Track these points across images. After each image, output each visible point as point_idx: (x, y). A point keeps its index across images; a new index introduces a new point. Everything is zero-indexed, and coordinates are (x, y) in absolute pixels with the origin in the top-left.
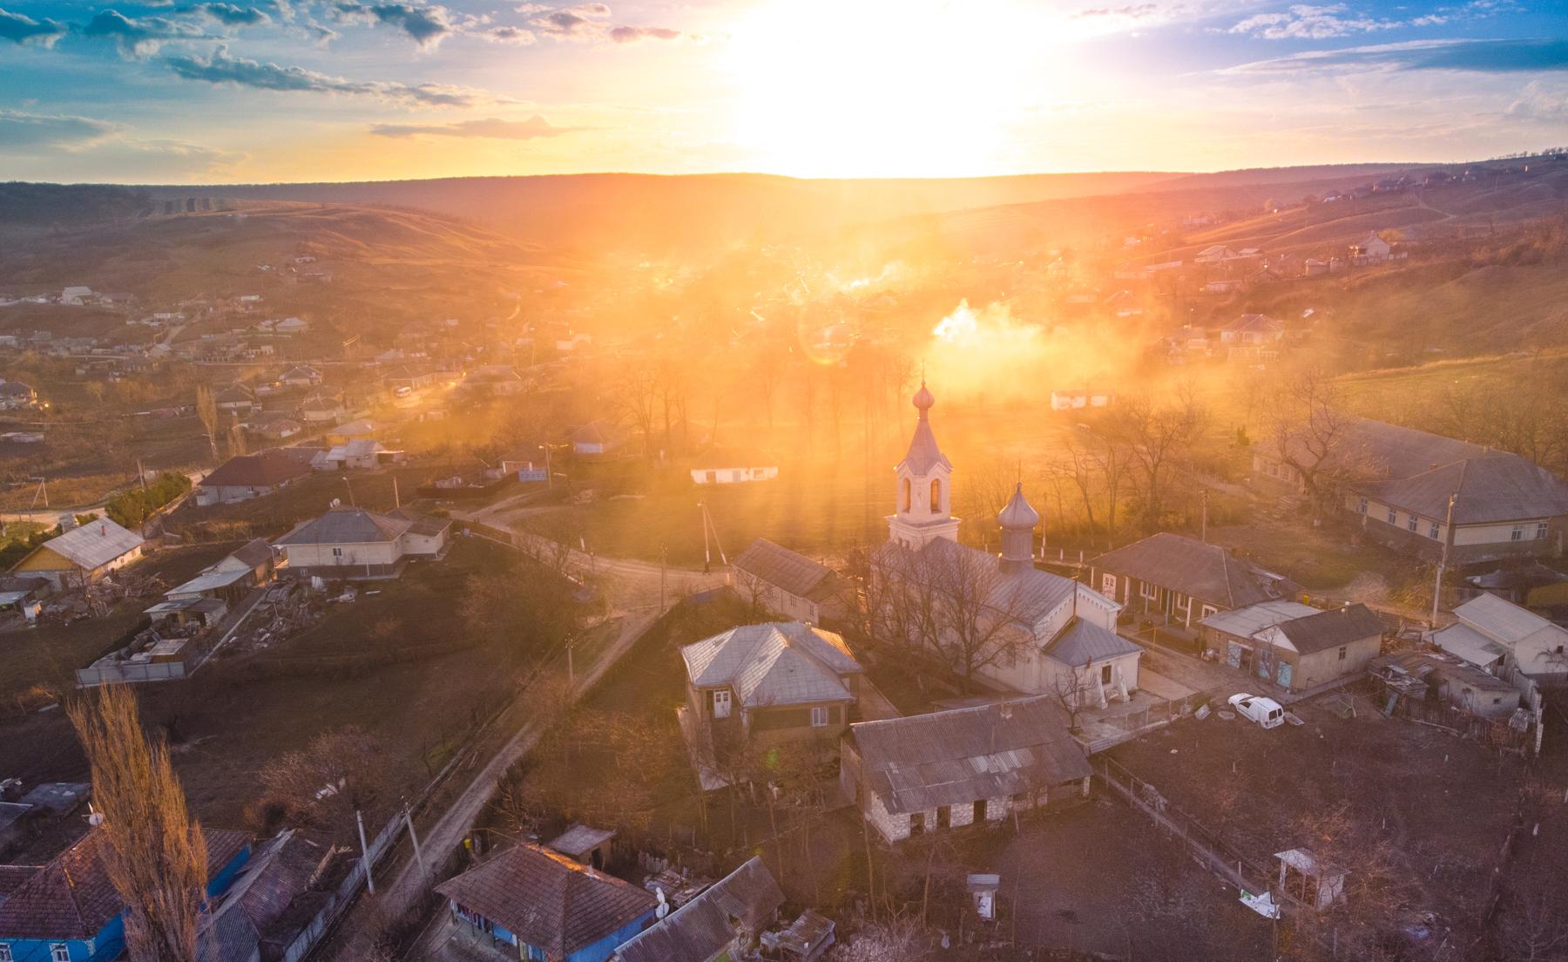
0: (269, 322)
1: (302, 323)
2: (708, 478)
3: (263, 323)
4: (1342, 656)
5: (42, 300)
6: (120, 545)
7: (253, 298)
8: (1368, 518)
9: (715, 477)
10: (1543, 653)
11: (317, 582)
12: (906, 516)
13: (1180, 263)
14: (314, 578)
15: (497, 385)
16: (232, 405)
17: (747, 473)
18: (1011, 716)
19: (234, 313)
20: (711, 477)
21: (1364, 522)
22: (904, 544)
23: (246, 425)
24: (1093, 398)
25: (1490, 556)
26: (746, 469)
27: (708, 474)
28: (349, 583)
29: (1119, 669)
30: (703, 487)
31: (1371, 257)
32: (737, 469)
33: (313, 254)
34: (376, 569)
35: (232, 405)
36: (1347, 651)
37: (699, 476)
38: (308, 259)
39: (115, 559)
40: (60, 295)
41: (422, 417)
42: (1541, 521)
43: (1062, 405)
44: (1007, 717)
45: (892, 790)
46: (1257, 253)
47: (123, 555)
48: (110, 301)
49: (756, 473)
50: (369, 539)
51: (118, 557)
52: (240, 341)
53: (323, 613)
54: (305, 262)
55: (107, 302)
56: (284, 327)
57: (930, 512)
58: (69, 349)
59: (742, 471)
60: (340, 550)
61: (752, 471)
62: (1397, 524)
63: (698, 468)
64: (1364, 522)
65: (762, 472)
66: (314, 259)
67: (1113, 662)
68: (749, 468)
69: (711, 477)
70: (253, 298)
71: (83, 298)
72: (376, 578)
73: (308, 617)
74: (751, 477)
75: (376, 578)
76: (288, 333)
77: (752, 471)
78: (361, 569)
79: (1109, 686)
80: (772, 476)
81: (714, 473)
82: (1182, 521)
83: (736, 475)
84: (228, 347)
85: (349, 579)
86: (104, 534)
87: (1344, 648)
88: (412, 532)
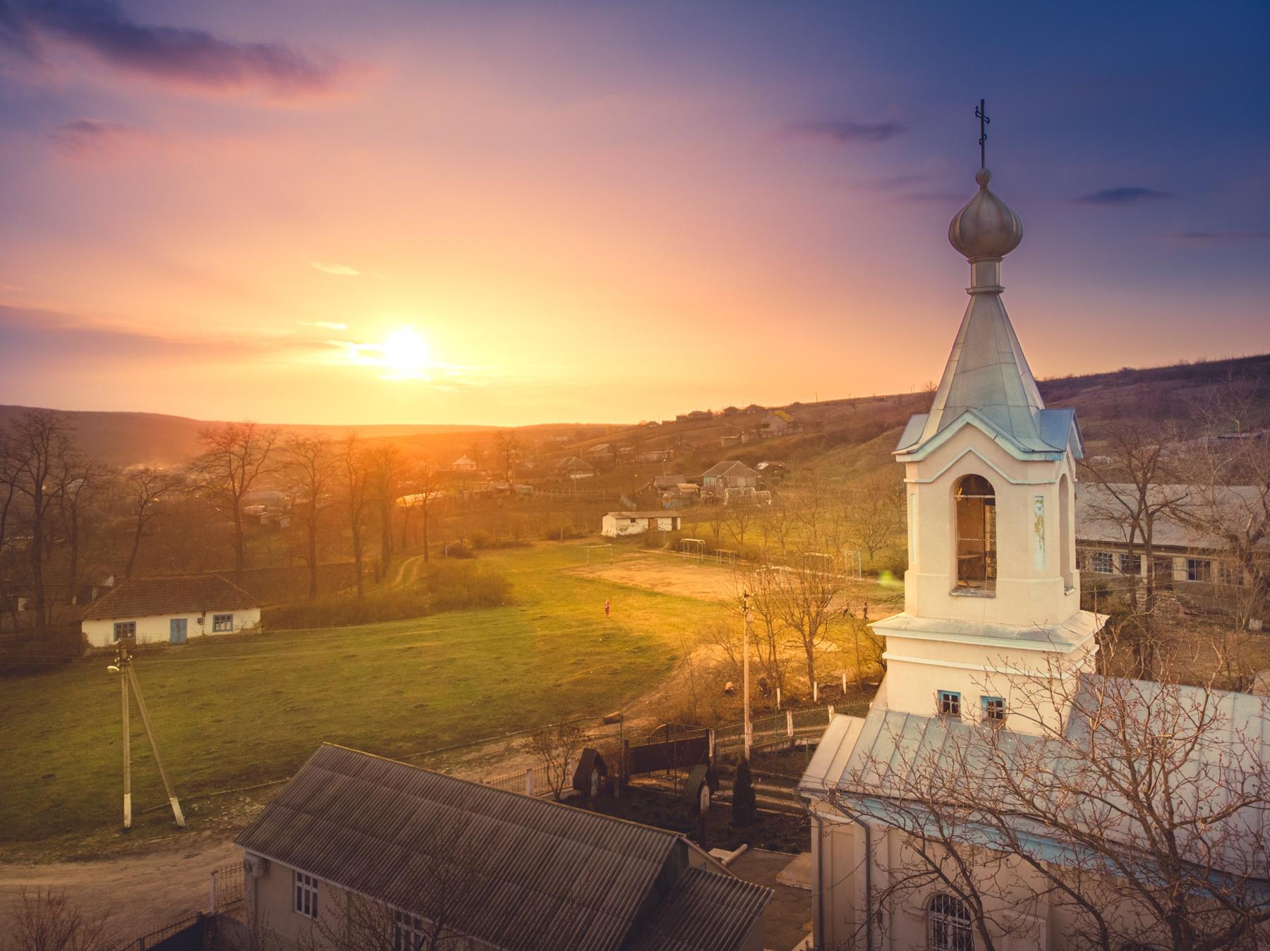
2: (118, 635)
9: (133, 631)
12: (973, 608)
17: (200, 621)
22: (971, 710)
26: (200, 616)
27: (118, 626)
30: (108, 654)
43: (621, 530)
49: (217, 620)
61: (209, 619)
63: (98, 617)
65: (229, 618)
68: (204, 614)
69: (125, 632)
74: (208, 628)
77: (209, 619)
80: (249, 625)
83: (178, 627)
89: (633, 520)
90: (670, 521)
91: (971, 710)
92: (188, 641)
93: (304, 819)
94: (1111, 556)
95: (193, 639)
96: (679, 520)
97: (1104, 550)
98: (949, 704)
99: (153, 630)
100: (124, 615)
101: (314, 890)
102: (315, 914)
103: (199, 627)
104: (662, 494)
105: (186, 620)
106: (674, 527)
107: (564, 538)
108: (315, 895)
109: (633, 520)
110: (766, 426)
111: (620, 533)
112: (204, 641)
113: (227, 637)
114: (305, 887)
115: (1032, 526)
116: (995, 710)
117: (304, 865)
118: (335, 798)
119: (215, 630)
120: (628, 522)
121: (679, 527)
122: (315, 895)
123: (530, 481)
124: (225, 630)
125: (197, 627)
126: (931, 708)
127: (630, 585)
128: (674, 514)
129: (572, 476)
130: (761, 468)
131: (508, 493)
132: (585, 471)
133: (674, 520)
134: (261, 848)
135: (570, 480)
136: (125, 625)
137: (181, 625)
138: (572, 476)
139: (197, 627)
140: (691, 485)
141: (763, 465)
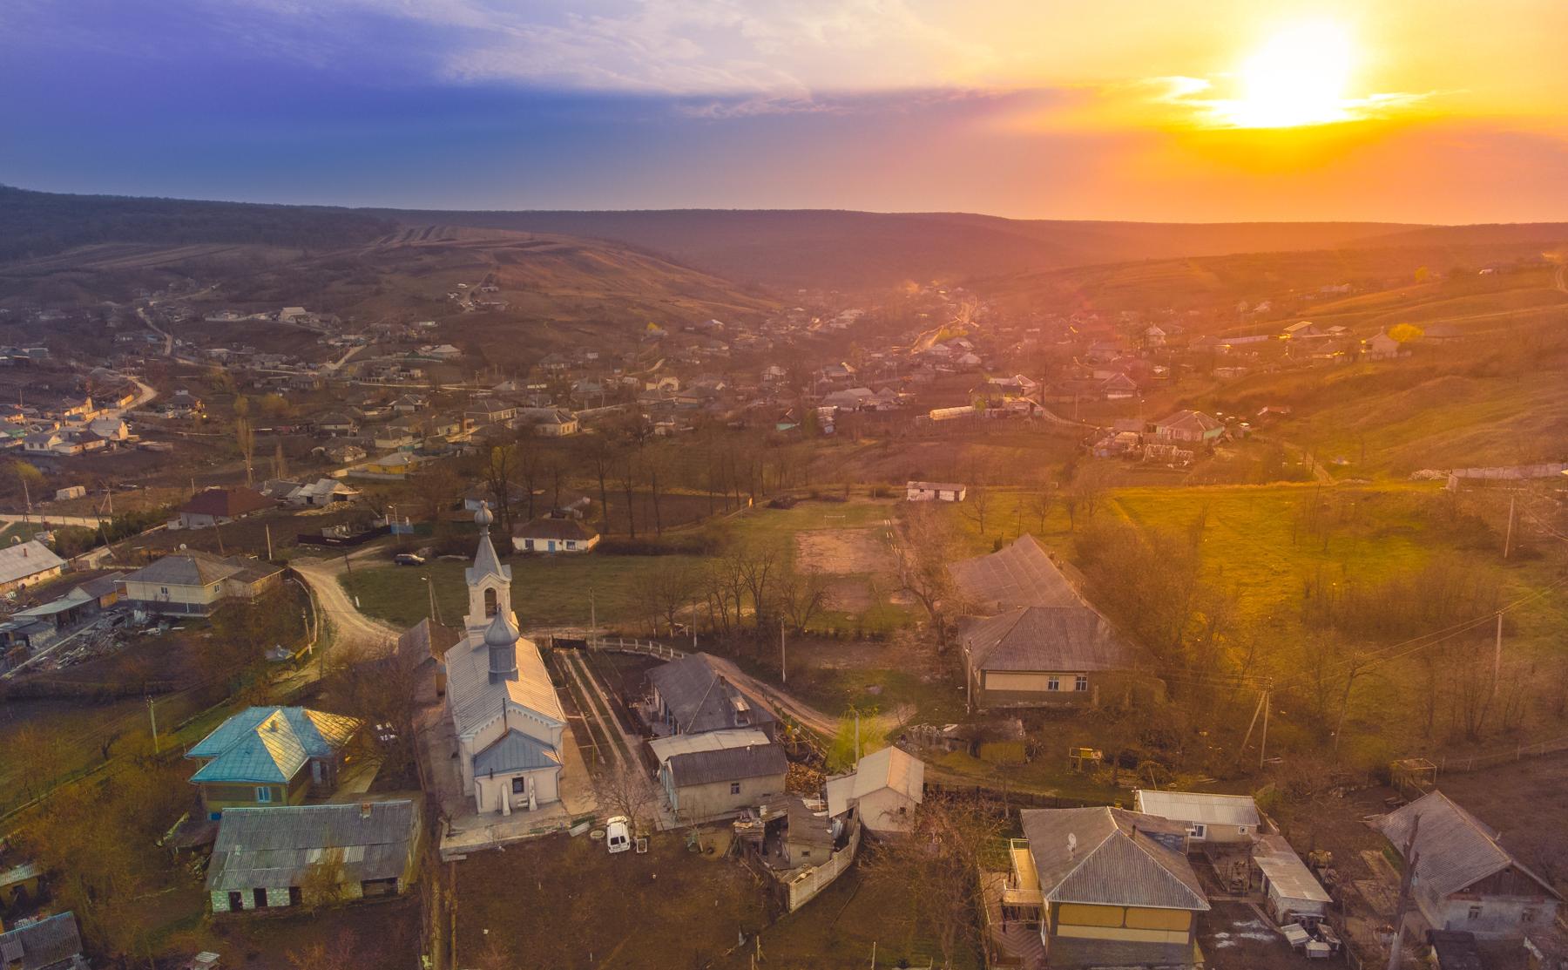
0: (429, 347)
1: (454, 349)
2: (527, 546)
3: (423, 349)
4: (736, 790)
5: (263, 317)
6: (36, 565)
7: (430, 324)
9: (533, 545)
10: (885, 812)
11: (139, 615)
14: (135, 611)
15: (539, 427)
16: (333, 427)
17: (561, 543)
18: (368, 816)
19: (407, 336)
20: (529, 544)
23: (323, 449)
24: (941, 492)
25: (1026, 703)
27: (526, 541)
28: (163, 617)
29: (531, 782)
30: (521, 553)
32: (551, 540)
33: (497, 284)
34: (195, 608)
35: (333, 427)
36: (741, 786)
38: (492, 288)
39: (28, 577)
40: (279, 314)
41: (459, 452)
42: (1081, 675)
44: (365, 817)
45: (222, 869)
46: (1343, 331)
47: (38, 573)
48: (317, 321)
50: (188, 582)
51: (31, 575)
52: (393, 365)
53: (127, 643)
54: (489, 290)
55: (315, 321)
56: (438, 353)
57: (485, 616)
58: (263, 363)
59: (557, 542)
60: (166, 589)
63: (519, 536)
65: (574, 543)
66: (497, 289)
67: (524, 774)
69: (529, 544)
70: (430, 324)
71: (297, 317)
72: (193, 615)
73: (110, 645)
75: (193, 615)
76: (441, 359)
77: (565, 543)
78: (180, 607)
79: (520, 797)
80: (583, 548)
81: (532, 541)
82: (831, 631)
83: (552, 545)
84: (384, 369)
85: (165, 614)
86: (26, 555)
87: (738, 784)
88: (235, 579)
90: (953, 494)
99: (541, 545)
103: (559, 546)
106: (957, 498)
112: (562, 554)
113: (572, 553)
125: (560, 546)
129: (1109, 396)
133: (957, 493)
135: (1107, 399)
138: (1109, 396)
139: (560, 546)
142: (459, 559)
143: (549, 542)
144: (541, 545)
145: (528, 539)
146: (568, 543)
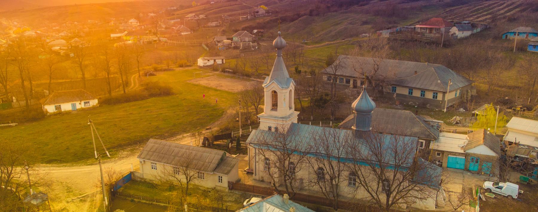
8: (397, 94)
9: (60, 108)
12: (274, 113)
13: (179, 20)
17: (80, 104)
21: (395, 96)
22: (273, 130)
26: (80, 102)
27: (56, 106)
30: (55, 114)
31: (261, 14)
37: (50, 109)
46: (205, 16)
61: (83, 103)
62: (414, 95)
63: (50, 103)
64: (395, 96)
65: (89, 102)
68: (81, 101)
74: (83, 105)
77: (83, 103)
80: (95, 104)
81: (60, 106)
83: (74, 105)
89: (208, 60)
90: (221, 60)
91: (273, 130)
92: (77, 110)
93: (150, 153)
94: (343, 79)
95: (79, 109)
96: (224, 60)
97: (342, 77)
98: (270, 128)
100: (57, 103)
101: (156, 165)
102: (156, 169)
104: (218, 44)
105: (76, 104)
106: (223, 62)
107: (185, 67)
108: (156, 166)
109: (208, 60)
110: (257, 12)
111: (204, 65)
112: (82, 110)
113: (89, 108)
114: (153, 165)
115: (283, 100)
116: (276, 129)
117: (154, 161)
118: (156, 149)
119: (85, 106)
120: (207, 61)
121: (224, 63)
122: (156, 166)
123: (166, 36)
124: (88, 106)
126: (267, 129)
127: (209, 87)
128: (222, 58)
129: (182, 34)
130: (255, 32)
131: (158, 41)
132: (187, 31)
133: (223, 60)
134: (144, 158)
135: (181, 35)
136: (58, 106)
137: (75, 105)
138: (182, 34)
140: (228, 41)
141: (255, 31)
142: (10, 126)
143: (72, 104)
144: (66, 107)
145: (72, 103)
146: (85, 103)
